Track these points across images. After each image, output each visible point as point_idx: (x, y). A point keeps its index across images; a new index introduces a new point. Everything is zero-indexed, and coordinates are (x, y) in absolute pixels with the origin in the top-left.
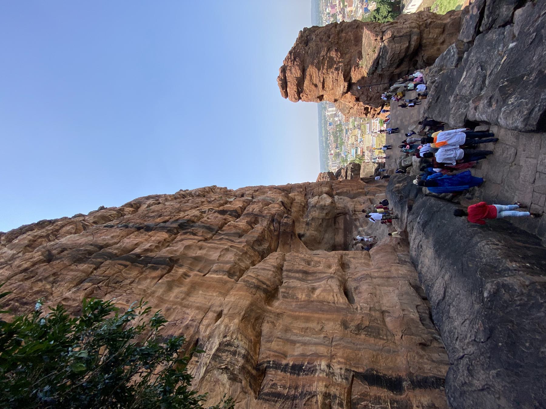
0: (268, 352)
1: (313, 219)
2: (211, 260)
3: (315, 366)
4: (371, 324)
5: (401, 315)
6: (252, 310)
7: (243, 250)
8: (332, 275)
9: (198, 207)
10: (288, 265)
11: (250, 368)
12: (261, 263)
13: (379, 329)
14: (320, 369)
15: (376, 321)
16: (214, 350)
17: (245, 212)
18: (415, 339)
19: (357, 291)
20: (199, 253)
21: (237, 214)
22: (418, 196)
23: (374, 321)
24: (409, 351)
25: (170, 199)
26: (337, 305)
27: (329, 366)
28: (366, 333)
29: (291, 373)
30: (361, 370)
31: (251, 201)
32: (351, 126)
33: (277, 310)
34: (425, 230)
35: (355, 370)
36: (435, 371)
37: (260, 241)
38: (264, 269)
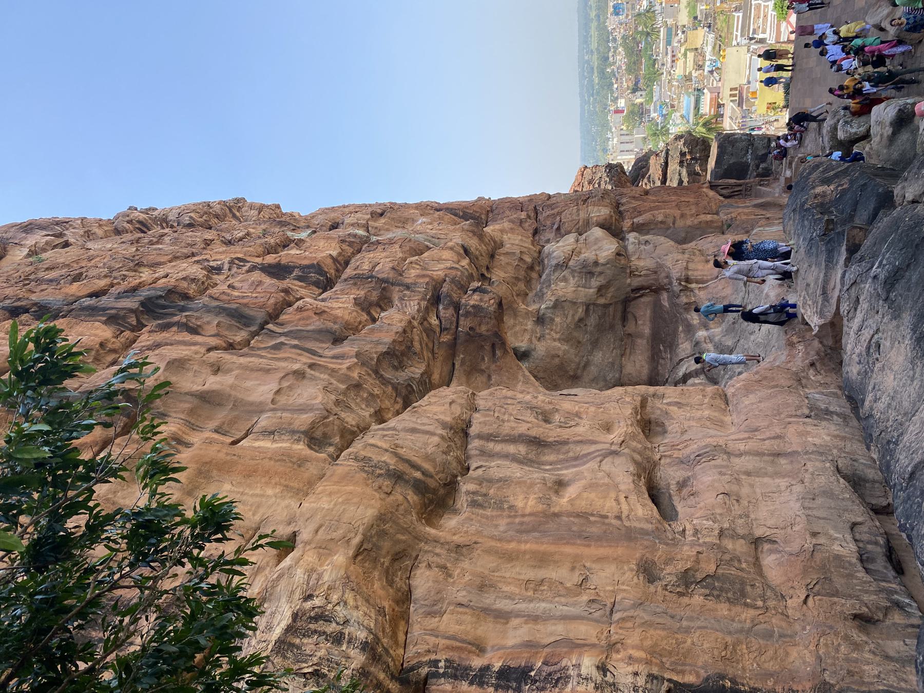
0: (432, 640)
1: (557, 305)
2: (252, 404)
3: (566, 668)
4: (720, 571)
5: (808, 546)
6: (382, 534)
7: (348, 378)
8: (614, 448)
9: (193, 255)
10: (485, 423)
11: (382, 676)
12: (405, 415)
13: (743, 583)
14: (579, 675)
15: (736, 564)
16: (277, 632)
17: (349, 272)
18: (843, 605)
19: (685, 491)
20: (212, 382)
21: (323, 279)
22: (881, 214)
23: (729, 562)
24: (824, 634)
25: (100, 232)
26: (627, 524)
27: (602, 669)
28: (707, 592)
29: (497, 687)
30: (690, 679)
31: (365, 241)
32: (684, 18)
33: (455, 538)
34: (892, 295)
35: (675, 678)
36: (892, 680)
37: (397, 355)
38: (413, 431)
